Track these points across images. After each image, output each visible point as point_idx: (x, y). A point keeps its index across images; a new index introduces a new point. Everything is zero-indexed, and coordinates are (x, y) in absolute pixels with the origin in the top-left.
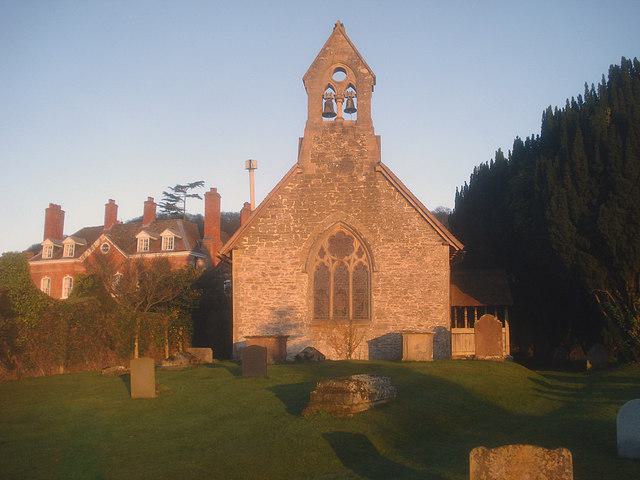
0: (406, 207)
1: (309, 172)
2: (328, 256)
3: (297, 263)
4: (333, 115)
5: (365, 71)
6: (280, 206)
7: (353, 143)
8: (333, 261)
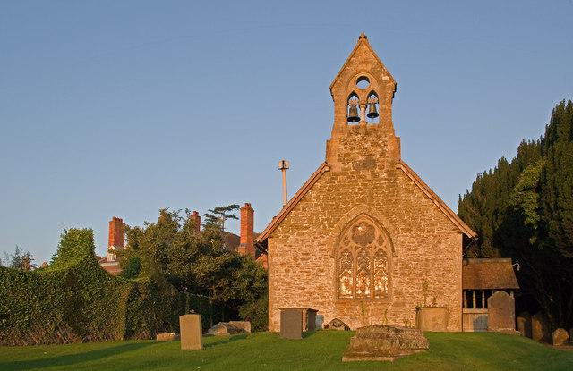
0: (423, 200)
1: (334, 170)
2: (352, 243)
3: (325, 250)
4: (357, 119)
5: (387, 78)
6: (310, 200)
7: (375, 144)
8: (357, 248)
